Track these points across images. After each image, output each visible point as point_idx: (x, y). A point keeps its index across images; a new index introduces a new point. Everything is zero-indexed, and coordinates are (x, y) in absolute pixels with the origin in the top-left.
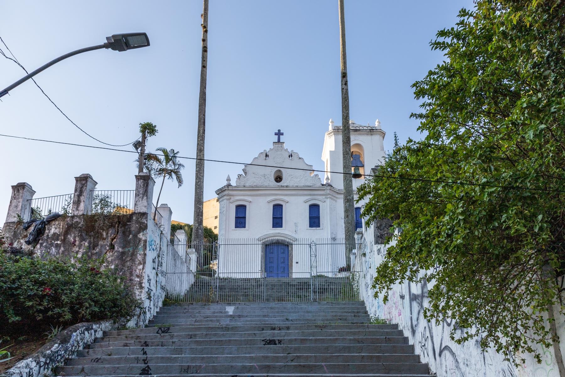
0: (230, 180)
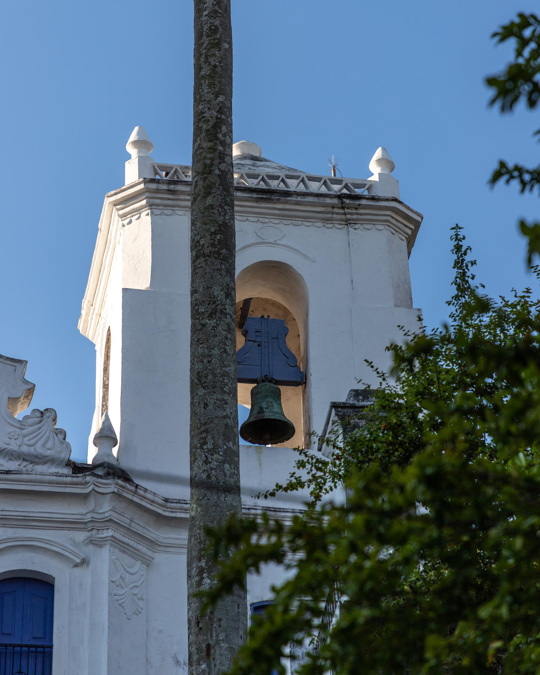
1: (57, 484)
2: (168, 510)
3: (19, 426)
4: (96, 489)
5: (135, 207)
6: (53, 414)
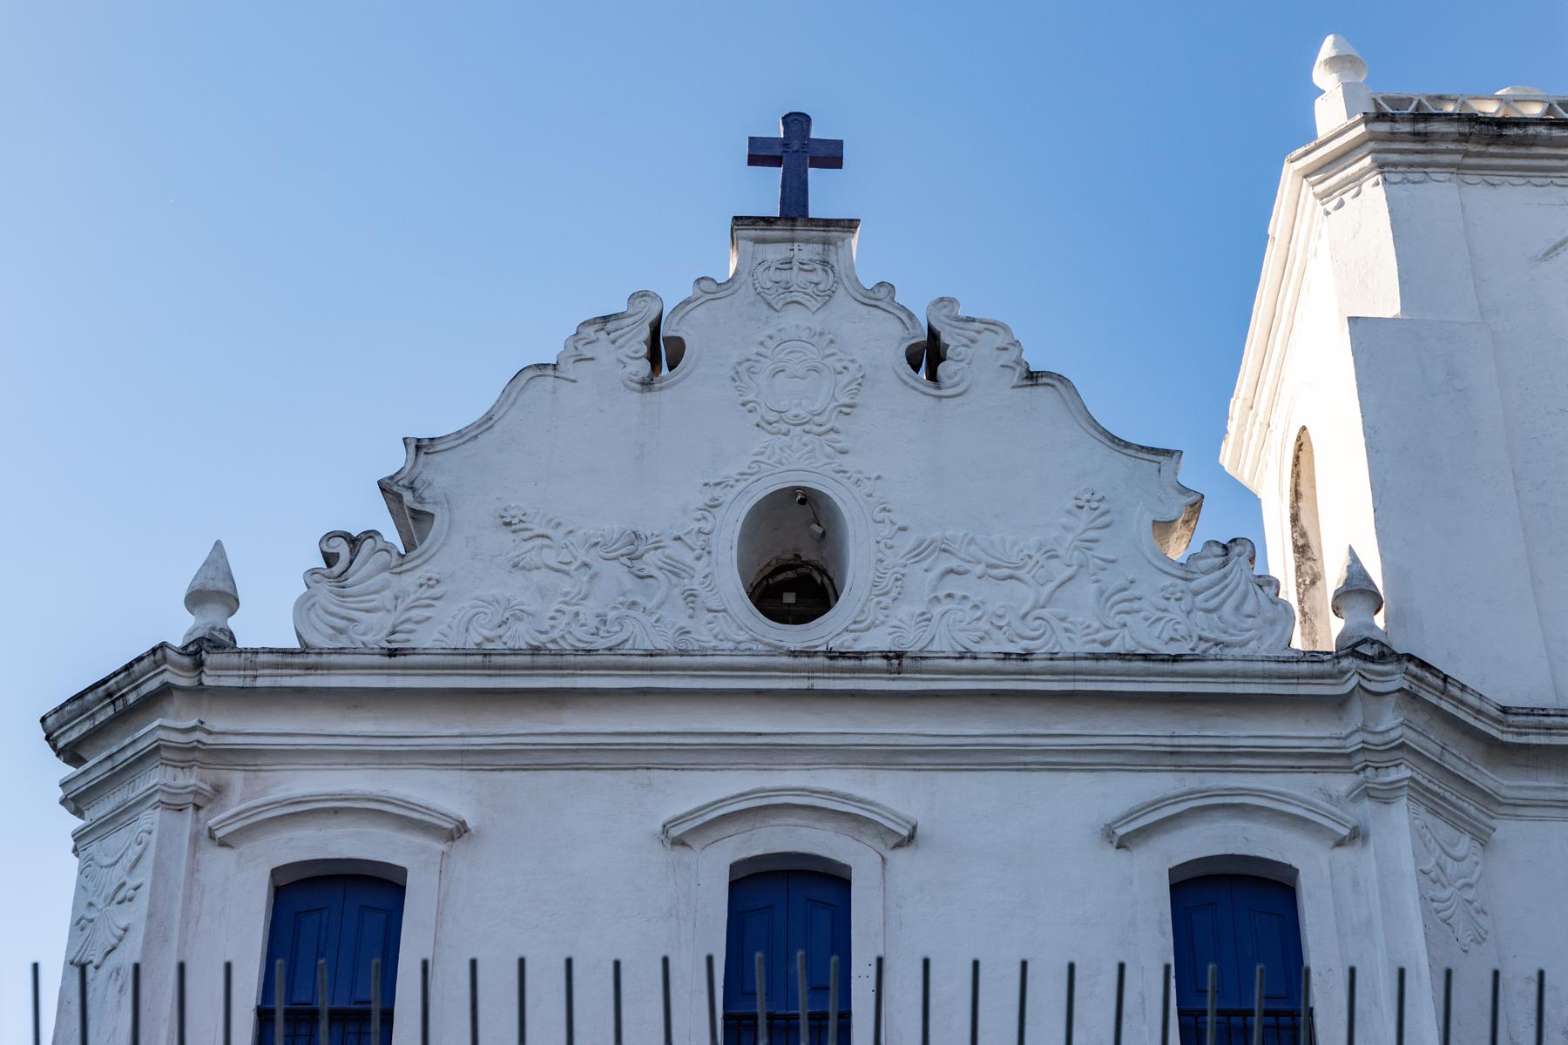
0: (230, 601)
1: (1279, 677)
2: (1511, 729)
4: (1365, 684)
5: (1350, 174)
6: (1249, 548)
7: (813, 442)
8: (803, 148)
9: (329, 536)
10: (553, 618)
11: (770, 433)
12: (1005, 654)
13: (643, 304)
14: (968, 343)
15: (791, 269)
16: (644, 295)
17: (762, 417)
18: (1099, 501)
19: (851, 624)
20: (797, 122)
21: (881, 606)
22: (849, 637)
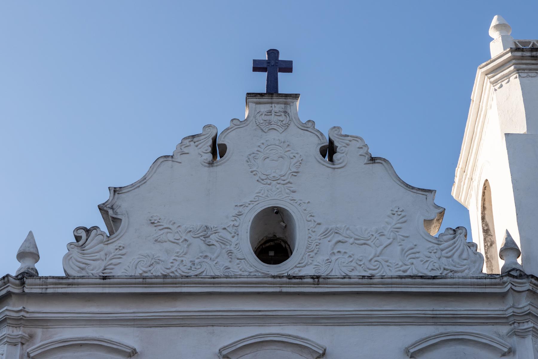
0: (36, 257)
1: (478, 285)
3: (436, 242)
4: (513, 287)
5: (505, 73)
6: (464, 231)
7: (281, 188)
8: (276, 64)
9: (77, 229)
10: (172, 263)
11: (263, 184)
12: (363, 276)
13: (209, 130)
14: (346, 145)
15: (271, 115)
16: (209, 126)
17: (260, 177)
18: (401, 211)
19: (298, 264)
20: (273, 53)
21: (311, 256)
22: (297, 269)
